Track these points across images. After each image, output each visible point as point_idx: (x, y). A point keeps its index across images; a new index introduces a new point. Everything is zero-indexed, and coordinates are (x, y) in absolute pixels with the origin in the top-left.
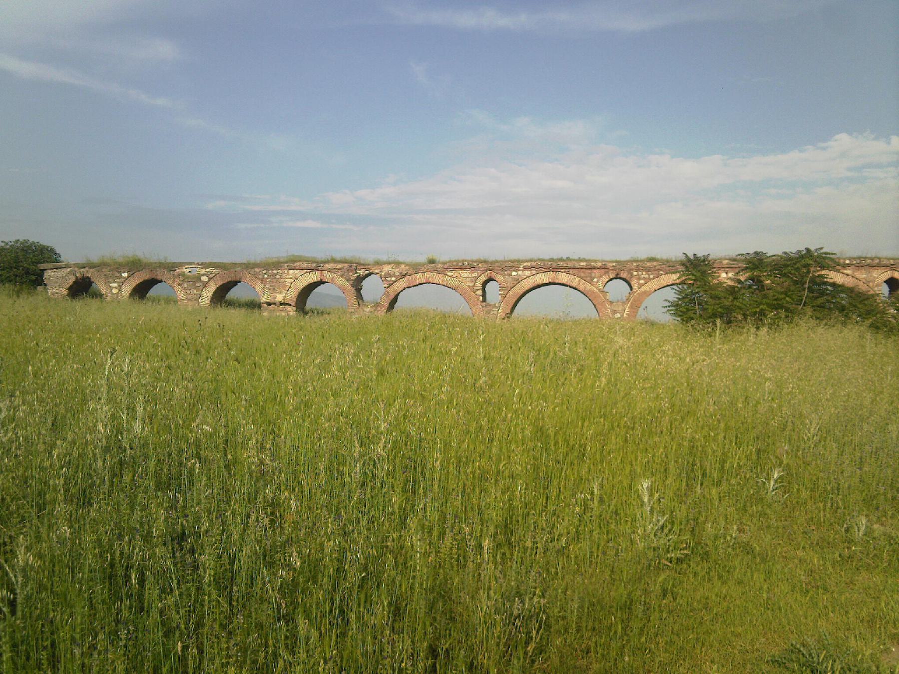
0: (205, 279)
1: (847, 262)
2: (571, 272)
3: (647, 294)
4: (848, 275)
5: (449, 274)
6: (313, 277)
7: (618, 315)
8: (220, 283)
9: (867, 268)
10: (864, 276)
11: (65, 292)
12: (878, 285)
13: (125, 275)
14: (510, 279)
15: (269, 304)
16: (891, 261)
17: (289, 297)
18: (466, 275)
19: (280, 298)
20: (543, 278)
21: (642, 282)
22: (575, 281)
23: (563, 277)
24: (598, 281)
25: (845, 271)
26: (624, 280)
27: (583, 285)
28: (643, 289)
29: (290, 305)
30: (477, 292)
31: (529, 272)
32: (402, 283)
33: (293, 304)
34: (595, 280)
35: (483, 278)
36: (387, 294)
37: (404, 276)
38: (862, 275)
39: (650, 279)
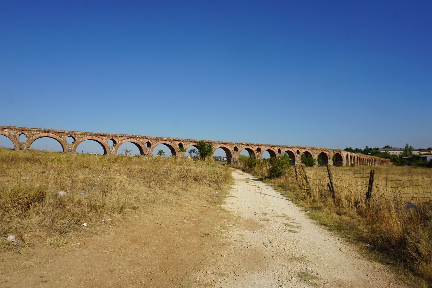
1: (138, 136)
2: (54, 133)
3: (80, 142)
5: (5, 130)
7: (70, 149)
9: (142, 139)
12: (145, 143)
14: (30, 134)
18: (12, 131)
20: (45, 134)
21: (79, 138)
22: (55, 136)
23: (51, 135)
24: (64, 137)
26: (73, 137)
27: (58, 138)
30: (17, 138)
31: (39, 132)
34: (63, 136)
35: (20, 133)
38: (141, 140)
39: (81, 137)
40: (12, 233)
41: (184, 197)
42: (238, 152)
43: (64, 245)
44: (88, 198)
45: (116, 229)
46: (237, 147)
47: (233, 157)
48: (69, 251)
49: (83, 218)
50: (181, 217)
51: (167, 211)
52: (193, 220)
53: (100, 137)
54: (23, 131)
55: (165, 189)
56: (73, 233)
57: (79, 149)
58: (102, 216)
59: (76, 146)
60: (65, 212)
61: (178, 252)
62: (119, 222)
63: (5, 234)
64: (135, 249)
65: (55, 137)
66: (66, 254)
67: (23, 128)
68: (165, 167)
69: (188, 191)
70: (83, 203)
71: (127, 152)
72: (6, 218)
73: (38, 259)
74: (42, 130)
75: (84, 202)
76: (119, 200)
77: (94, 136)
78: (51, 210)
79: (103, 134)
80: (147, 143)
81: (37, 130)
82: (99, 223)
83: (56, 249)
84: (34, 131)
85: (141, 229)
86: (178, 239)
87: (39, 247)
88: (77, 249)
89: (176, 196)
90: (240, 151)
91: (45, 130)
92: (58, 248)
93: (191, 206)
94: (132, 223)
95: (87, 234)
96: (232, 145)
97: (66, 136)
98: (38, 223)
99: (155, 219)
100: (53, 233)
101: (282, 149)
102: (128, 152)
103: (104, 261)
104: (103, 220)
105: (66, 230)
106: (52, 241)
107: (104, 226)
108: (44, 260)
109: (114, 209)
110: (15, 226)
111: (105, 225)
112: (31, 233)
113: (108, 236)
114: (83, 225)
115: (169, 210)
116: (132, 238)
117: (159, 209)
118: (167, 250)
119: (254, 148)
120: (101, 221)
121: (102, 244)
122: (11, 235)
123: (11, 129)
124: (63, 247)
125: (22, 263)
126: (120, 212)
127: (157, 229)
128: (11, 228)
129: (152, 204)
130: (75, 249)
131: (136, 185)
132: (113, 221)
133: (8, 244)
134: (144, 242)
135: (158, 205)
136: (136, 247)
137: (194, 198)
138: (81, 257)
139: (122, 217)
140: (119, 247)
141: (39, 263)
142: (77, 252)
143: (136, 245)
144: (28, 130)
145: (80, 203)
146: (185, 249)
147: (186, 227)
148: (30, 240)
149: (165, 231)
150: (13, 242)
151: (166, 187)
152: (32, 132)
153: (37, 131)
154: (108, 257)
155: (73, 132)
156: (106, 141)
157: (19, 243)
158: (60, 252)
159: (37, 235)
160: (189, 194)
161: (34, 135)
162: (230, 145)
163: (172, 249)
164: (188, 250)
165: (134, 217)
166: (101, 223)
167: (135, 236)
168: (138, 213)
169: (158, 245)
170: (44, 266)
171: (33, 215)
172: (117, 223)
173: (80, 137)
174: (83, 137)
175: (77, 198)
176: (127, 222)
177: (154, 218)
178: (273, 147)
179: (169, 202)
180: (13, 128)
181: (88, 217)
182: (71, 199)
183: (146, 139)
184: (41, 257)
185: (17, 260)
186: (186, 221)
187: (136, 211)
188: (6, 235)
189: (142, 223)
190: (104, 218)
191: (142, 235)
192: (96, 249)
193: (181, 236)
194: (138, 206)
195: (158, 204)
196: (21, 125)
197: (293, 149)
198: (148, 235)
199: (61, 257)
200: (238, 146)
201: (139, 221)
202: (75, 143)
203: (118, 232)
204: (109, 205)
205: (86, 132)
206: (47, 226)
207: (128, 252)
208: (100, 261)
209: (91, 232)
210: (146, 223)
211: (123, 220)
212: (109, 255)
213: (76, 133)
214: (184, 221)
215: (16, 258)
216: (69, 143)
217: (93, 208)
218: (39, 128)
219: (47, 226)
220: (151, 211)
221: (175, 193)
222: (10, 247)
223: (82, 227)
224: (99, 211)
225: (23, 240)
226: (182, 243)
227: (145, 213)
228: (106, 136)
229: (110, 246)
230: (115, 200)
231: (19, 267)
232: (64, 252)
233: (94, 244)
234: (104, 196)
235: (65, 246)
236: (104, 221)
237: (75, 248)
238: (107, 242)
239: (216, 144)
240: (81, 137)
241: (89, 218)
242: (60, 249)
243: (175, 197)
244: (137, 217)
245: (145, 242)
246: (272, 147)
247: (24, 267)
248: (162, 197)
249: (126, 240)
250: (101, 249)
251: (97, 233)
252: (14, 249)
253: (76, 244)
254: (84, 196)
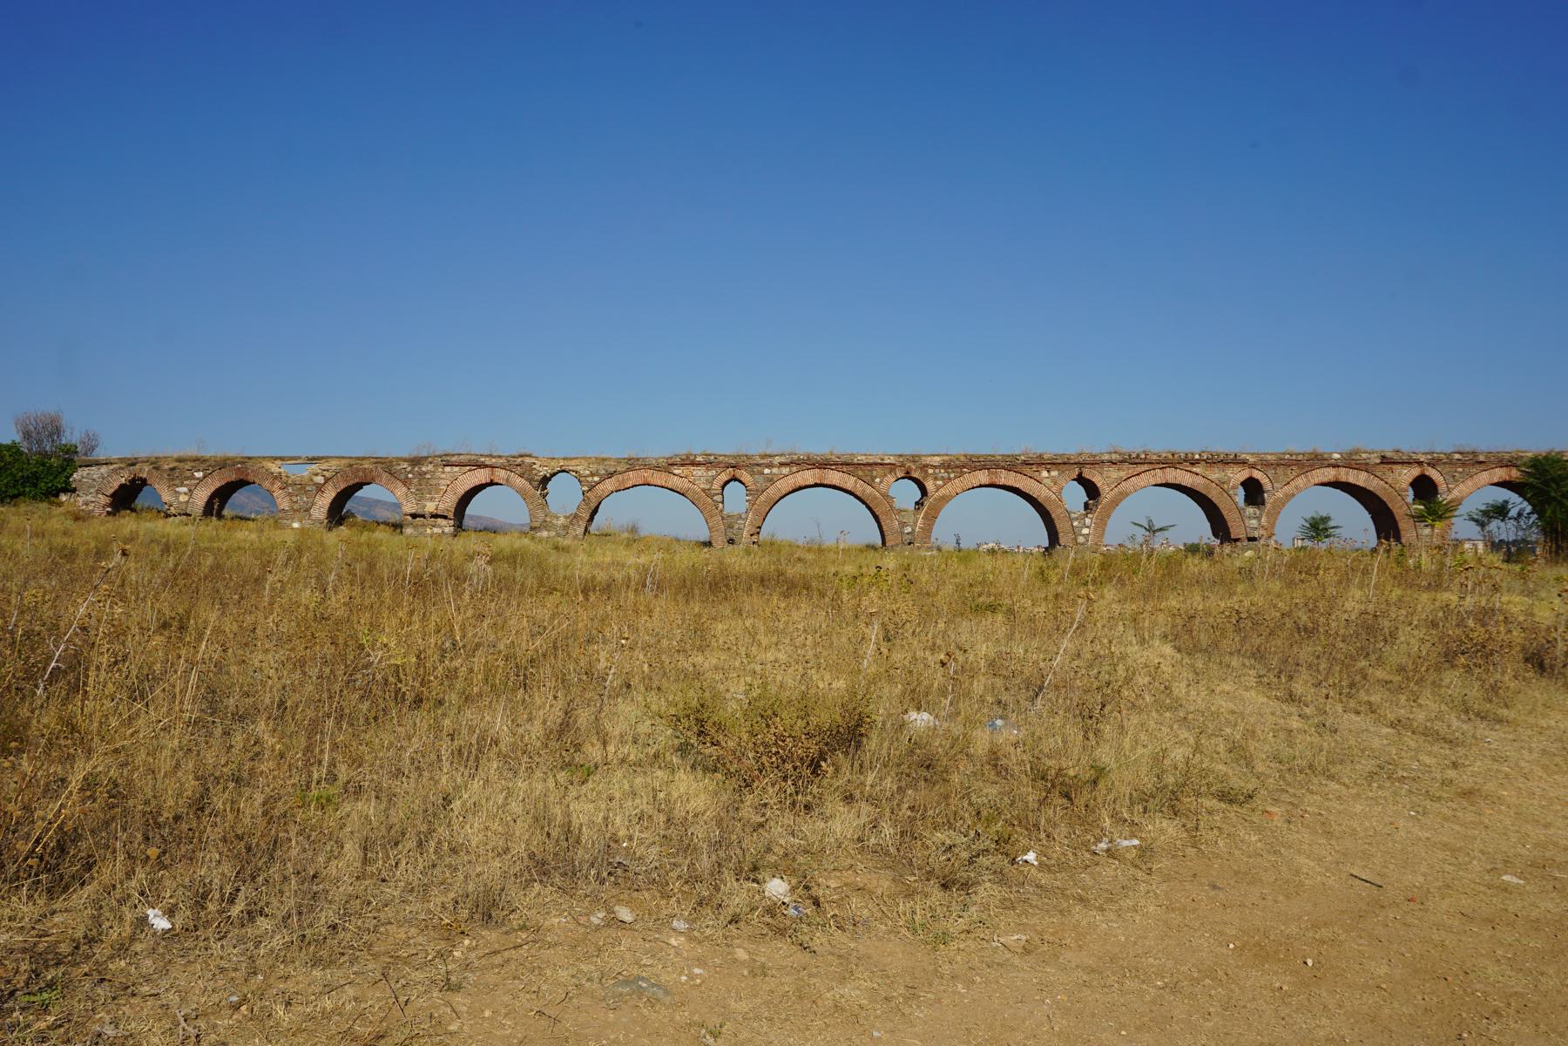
0: (320, 479)
1: (1197, 457)
3: (945, 499)
5: (676, 472)
6: (481, 476)
7: (909, 529)
8: (343, 486)
9: (1220, 465)
11: (103, 500)
12: (1234, 488)
13: (199, 475)
14: (760, 479)
15: (414, 516)
17: (441, 506)
18: (700, 473)
19: (430, 507)
20: (809, 476)
21: (940, 483)
22: (850, 482)
23: (834, 477)
24: (881, 482)
28: (942, 492)
29: (445, 517)
30: (715, 498)
32: (609, 485)
33: (451, 515)
34: (878, 480)
35: (724, 477)
36: (586, 500)
37: (610, 475)
38: (1215, 474)
39: (950, 479)
40: (776, 871)
41: (1484, 756)
43: (963, 936)
44: (1024, 745)
45: (1164, 887)
48: (989, 967)
49: (1018, 829)
50: (1484, 858)
51: (1401, 823)
52: (1556, 879)
53: (1027, 470)
54: (734, 468)
55: (1372, 712)
56: (987, 890)
57: (945, 530)
58: (1096, 823)
59: (931, 518)
60: (947, 797)
61: (1500, 1032)
62: (1174, 856)
63: (753, 872)
64: (1273, 991)
65: (849, 486)
66: (978, 974)
67: (734, 457)
68: (1354, 601)
69: (1500, 721)
70: (1010, 764)
71: (1154, 532)
72: (747, 812)
73: (880, 981)
74: (799, 459)
75: (1015, 759)
76: (1158, 759)
77: (1003, 468)
78: (895, 787)
79: (1040, 456)
80: (1243, 484)
81: (783, 460)
82: (1088, 855)
83: (935, 949)
84: (770, 466)
85: (1281, 898)
86: (1492, 969)
87: (876, 935)
88: (1017, 961)
89: (1436, 748)
91: (809, 459)
92: (942, 946)
93: (1535, 802)
94: (1236, 868)
95: (1047, 900)
97: (890, 478)
98: (856, 837)
99: (1344, 854)
100: (915, 881)
102: (1157, 534)
103: (1139, 1029)
104: (1103, 846)
105: (962, 875)
106: (918, 918)
107: (1109, 870)
108: (902, 990)
109: (1143, 799)
110: (782, 842)
111: (1113, 866)
112: (839, 874)
113: (1138, 919)
114: (1025, 858)
115: (1412, 817)
116: (1246, 939)
117: (1358, 808)
118: (1436, 1017)
120: (1094, 847)
121: (1117, 951)
122: (774, 876)
123: (693, 464)
124: (962, 946)
125: (828, 991)
126: (1171, 812)
127: (1364, 908)
128: (769, 850)
129: (1315, 781)
130: (1008, 960)
131: (1227, 687)
132: (1145, 852)
133: (771, 911)
134: (1310, 962)
135: (1348, 787)
136: (1278, 985)
137: (1545, 761)
138: (1037, 998)
139: (1185, 835)
140: (1196, 975)
141: (886, 998)
142: (1021, 975)
143: (1276, 973)
144: (752, 465)
145: (996, 766)
146: (1543, 1027)
147: (1525, 913)
148: (839, 904)
149: (1409, 919)
150: (784, 903)
151: (1375, 699)
152: (767, 471)
153: (782, 464)
154: (1153, 1015)
155: (914, 458)
156: (1054, 489)
157: (805, 911)
158: (955, 966)
159: (861, 885)
160: (1511, 737)
161: (771, 480)
163: (1464, 1015)
164: (1561, 1035)
165: (1242, 841)
166: (1096, 858)
167: (1262, 930)
168: (1255, 820)
169: (1384, 986)
170: (903, 1014)
171: (834, 805)
172: (1163, 863)
173: (942, 478)
174: (955, 477)
175: (981, 741)
176: (1209, 859)
177: (1337, 848)
179: (1405, 774)
180: (699, 459)
181: (1037, 826)
182: (961, 747)
183: (1236, 468)
184: (888, 977)
185: (810, 975)
186: (1515, 880)
187: (1244, 811)
188: (760, 877)
189: (1284, 869)
190: (1105, 835)
191: (1293, 929)
192: (1093, 971)
193: (1500, 952)
194: (1251, 787)
195: (1347, 781)
196: (725, 447)
198: (1324, 933)
199: (960, 986)
201: (1269, 861)
202: (927, 504)
203: (1177, 905)
204: (1122, 782)
205: (965, 456)
206: (888, 851)
207: (1242, 1003)
208: (1124, 1026)
209: (1063, 890)
210: (1305, 870)
211: (1191, 851)
212: (1154, 1002)
213: (928, 460)
214: (1505, 878)
215: (804, 969)
216: (903, 507)
217: (1060, 788)
218: (787, 451)
219: (887, 854)
220: (1320, 814)
221: (1429, 734)
222: (775, 920)
223: (1022, 869)
224: (1080, 801)
225: (817, 903)
226: (1515, 990)
227: (1289, 822)
228: (1052, 464)
229: (1153, 966)
230: (1142, 755)
231: (819, 1002)
232: (970, 968)
233: (1080, 946)
234: (1091, 735)
235: (969, 942)
236: (1108, 850)
237: (1008, 955)
238: (1135, 943)
240: (950, 479)
241: (1042, 828)
242: (952, 954)
243: (1430, 754)
244: (1253, 839)
245: (1317, 962)
247: (836, 1006)
248: (1363, 751)
249: (1222, 946)
250: (1114, 973)
251: (1088, 901)
252: (791, 931)
253: (1013, 939)
254: (1008, 734)
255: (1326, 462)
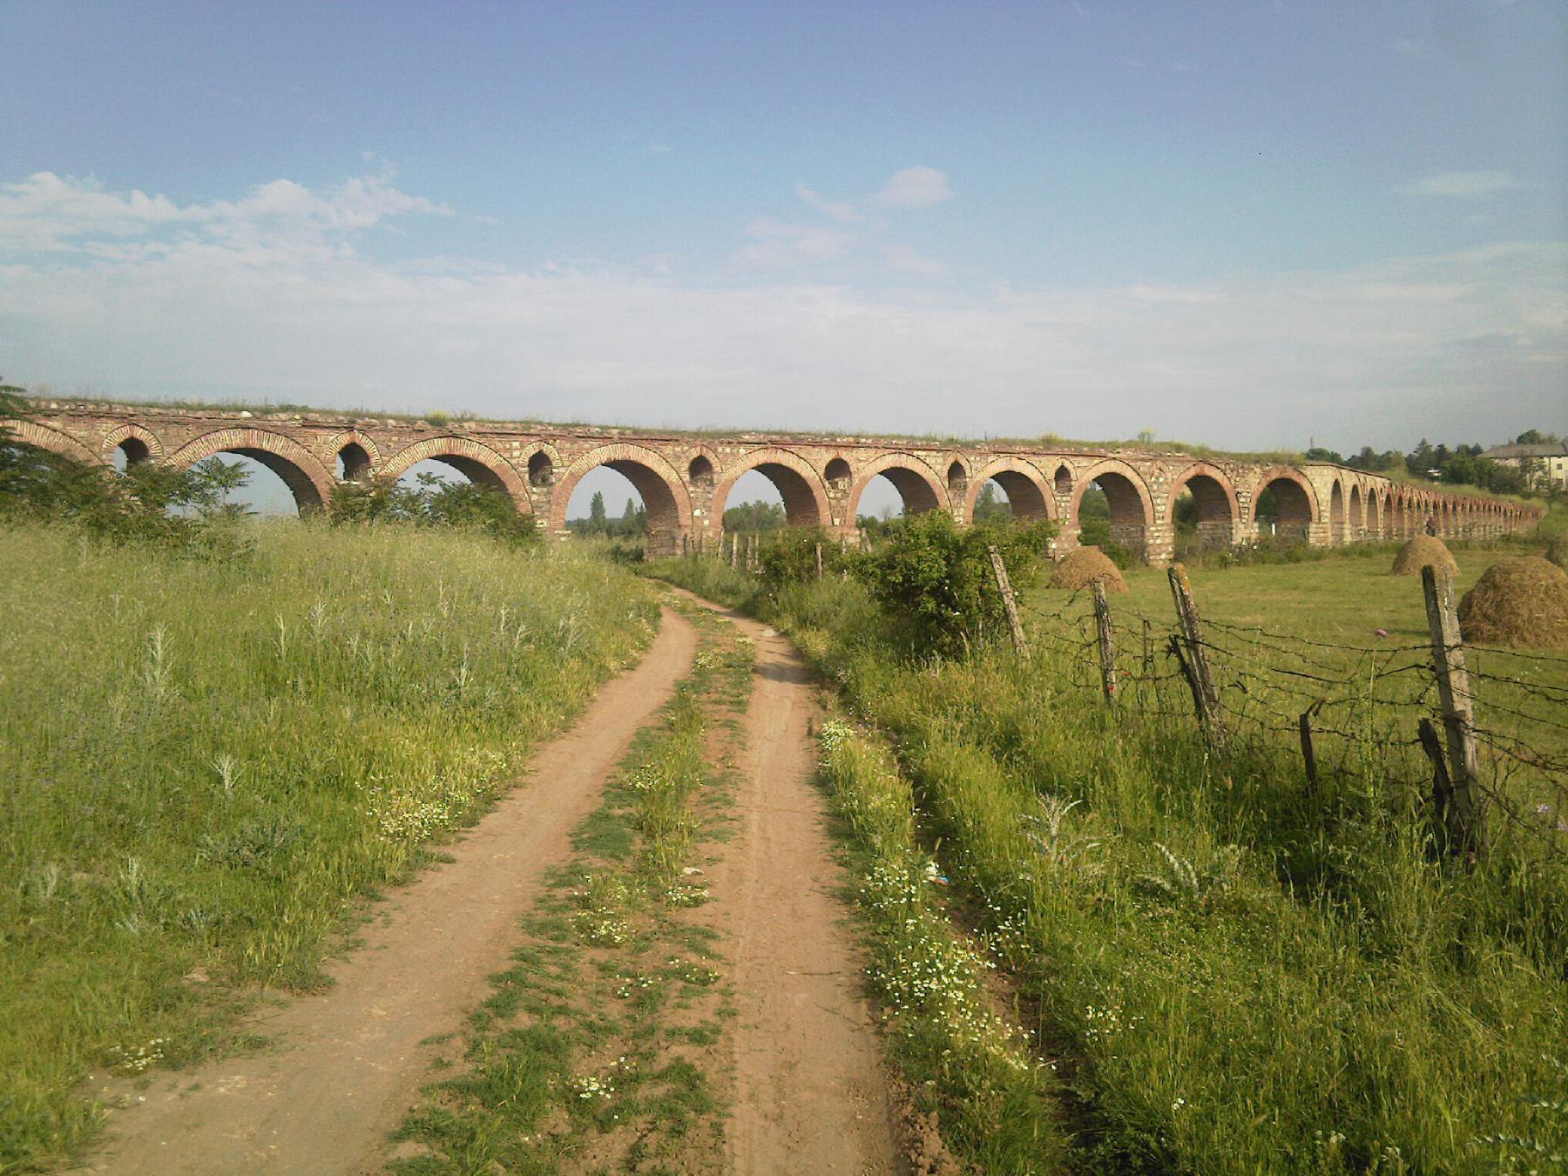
1: (54, 406)
4: (55, 431)
10: (82, 434)
12: (109, 451)
16: (130, 408)
25: (50, 423)
38: (79, 431)
42: (716, 491)
46: (711, 457)
47: (684, 519)
80: (122, 445)
90: (726, 480)
96: (678, 449)
101: (973, 464)
119: (811, 458)
162: (668, 450)
178: (919, 453)
183: (110, 424)
197: (1033, 459)
200: (715, 451)
239: (581, 442)
246: (915, 453)
255: (234, 423)
